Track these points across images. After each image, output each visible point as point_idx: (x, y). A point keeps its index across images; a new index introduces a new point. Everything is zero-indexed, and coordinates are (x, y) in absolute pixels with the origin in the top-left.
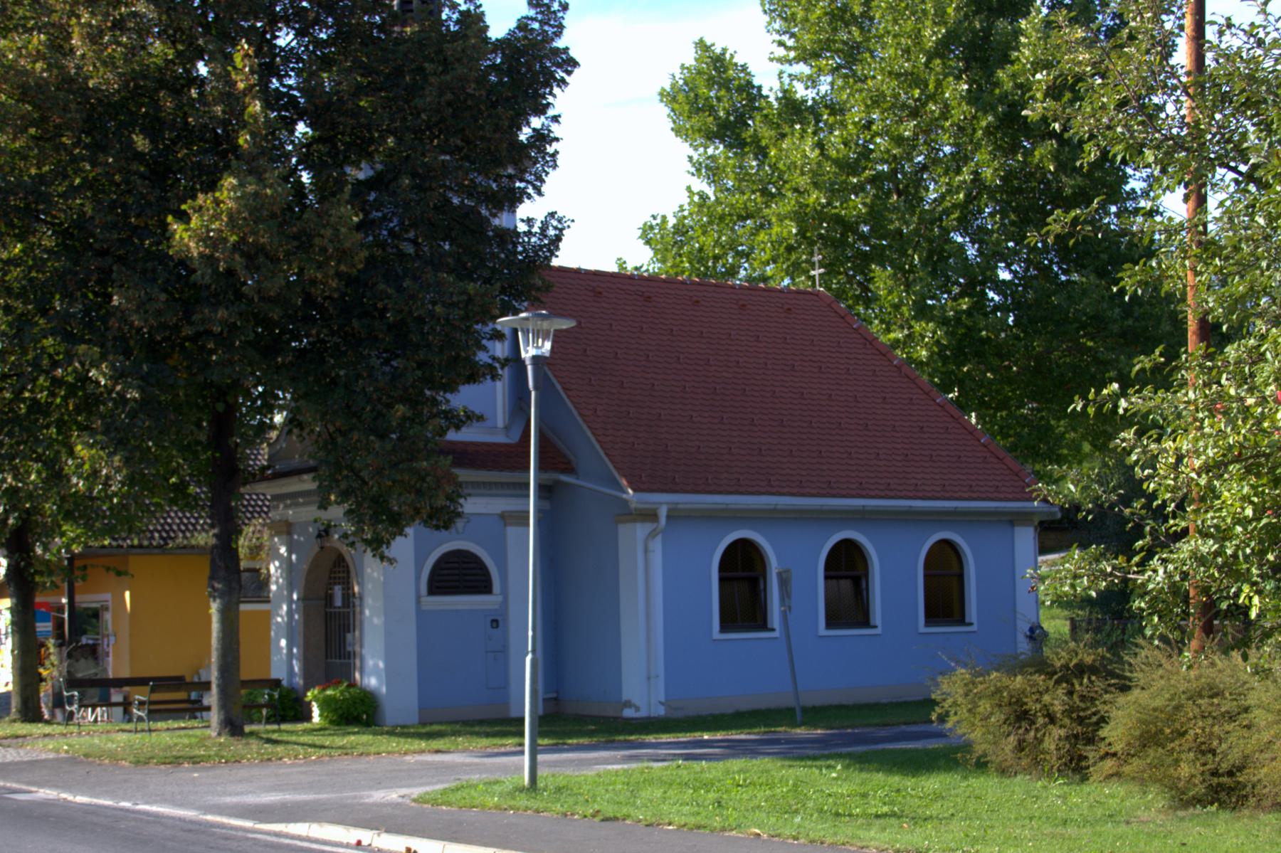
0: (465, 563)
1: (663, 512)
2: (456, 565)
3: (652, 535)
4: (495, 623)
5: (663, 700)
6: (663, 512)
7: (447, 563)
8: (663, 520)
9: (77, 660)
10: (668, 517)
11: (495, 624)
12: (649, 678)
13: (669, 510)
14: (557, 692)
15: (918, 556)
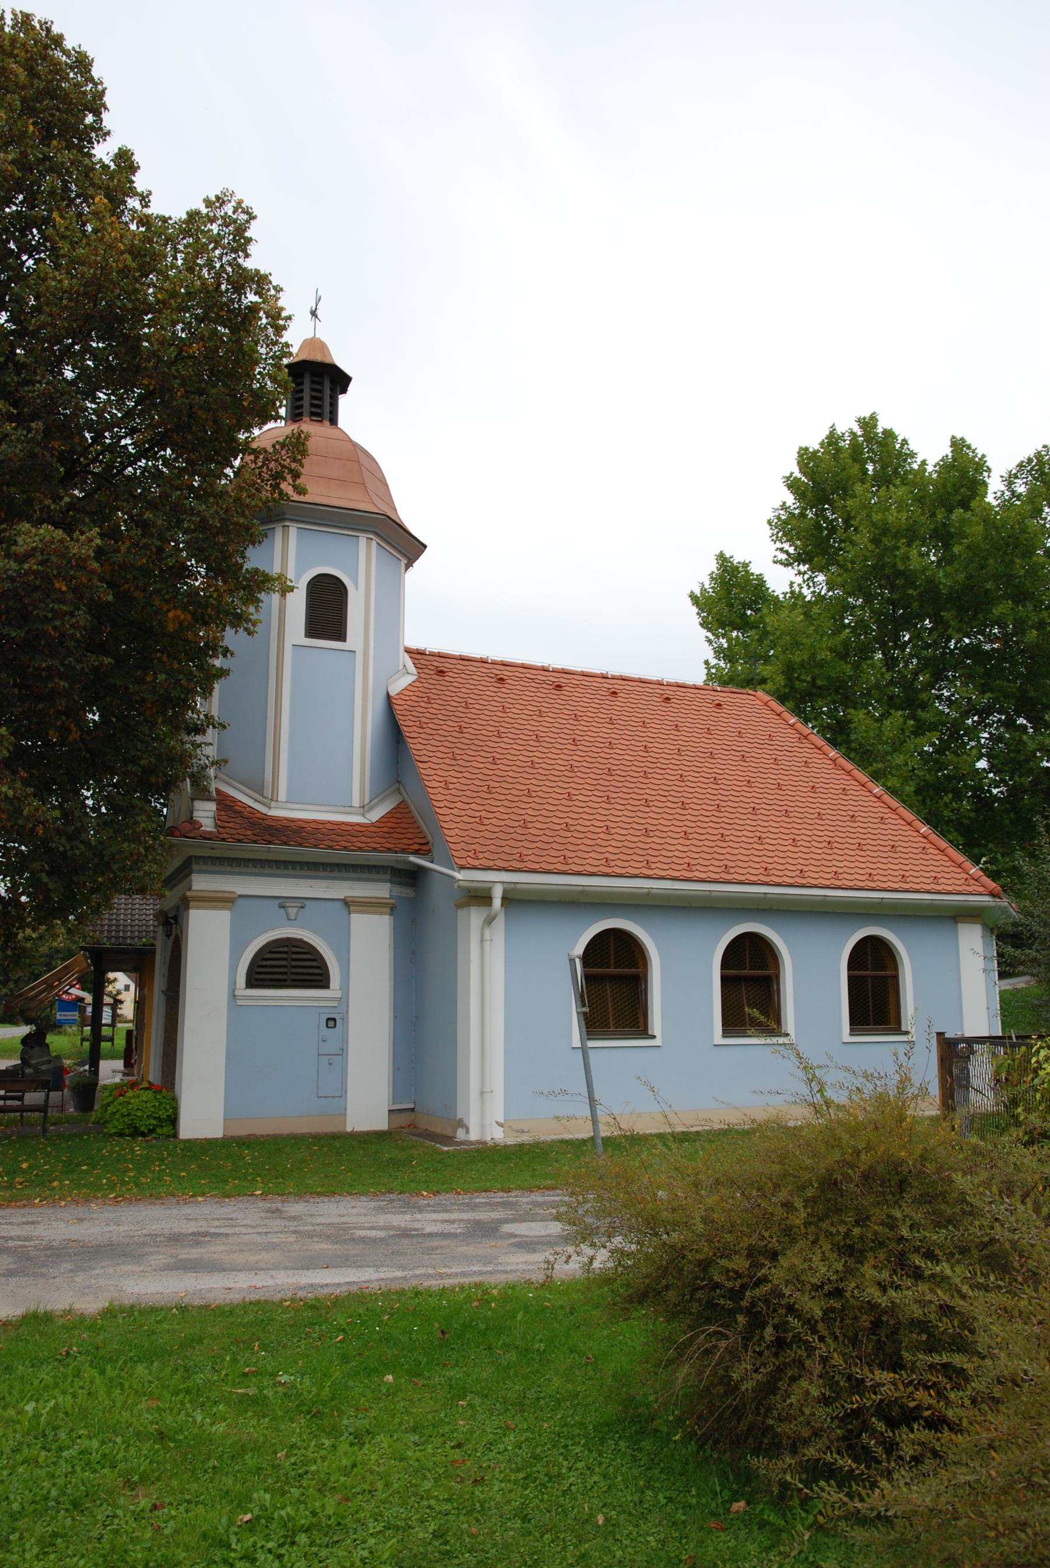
0: (294, 953)
1: (498, 893)
2: (285, 956)
3: (489, 921)
4: (331, 1022)
5: (502, 1121)
6: (498, 893)
7: (271, 952)
8: (497, 902)
9: (32, 1048)
10: (503, 899)
11: (331, 1023)
12: (482, 1093)
13: (505, 891)
14: (414, 1103)
15: (315, 931)
